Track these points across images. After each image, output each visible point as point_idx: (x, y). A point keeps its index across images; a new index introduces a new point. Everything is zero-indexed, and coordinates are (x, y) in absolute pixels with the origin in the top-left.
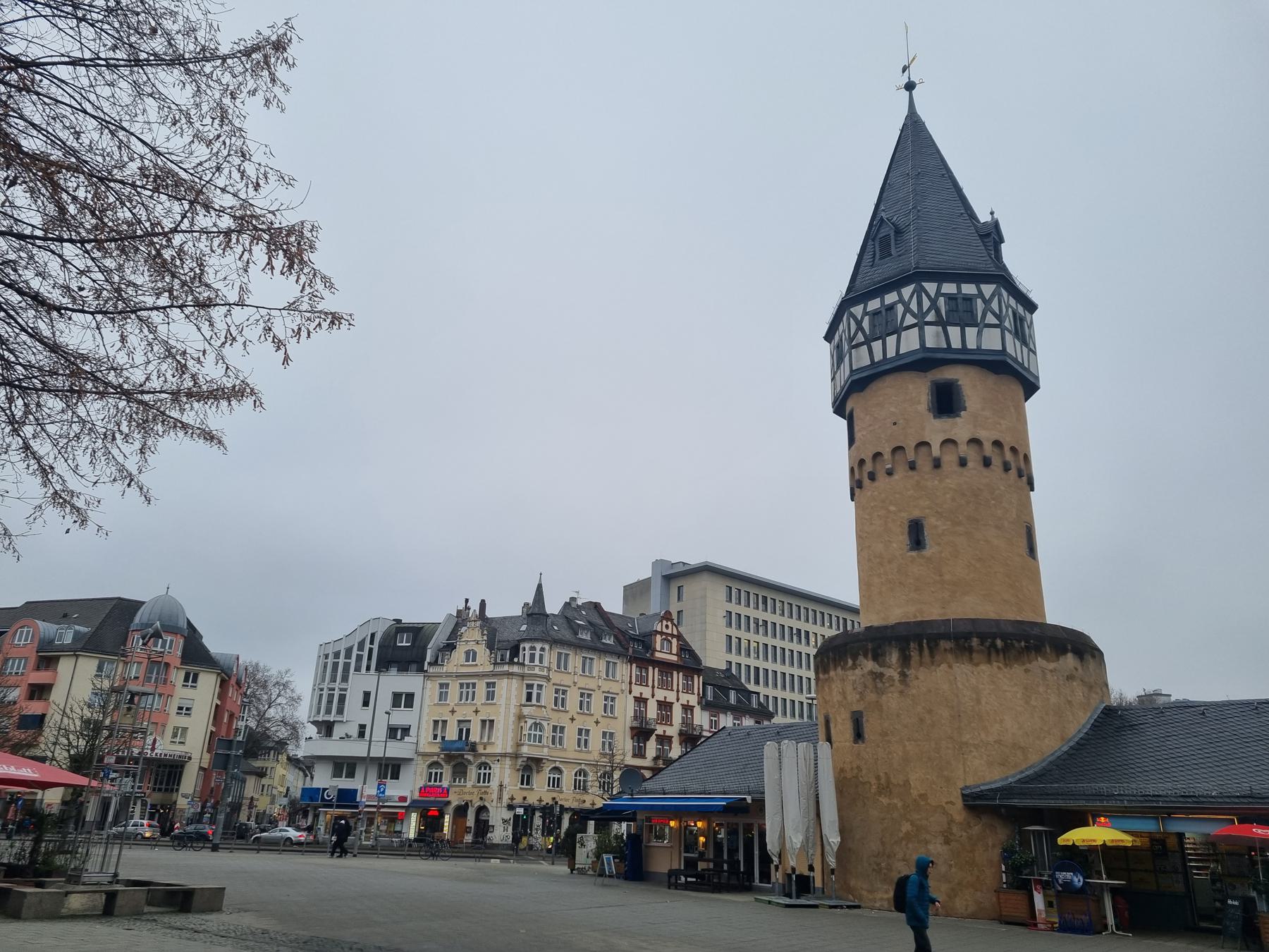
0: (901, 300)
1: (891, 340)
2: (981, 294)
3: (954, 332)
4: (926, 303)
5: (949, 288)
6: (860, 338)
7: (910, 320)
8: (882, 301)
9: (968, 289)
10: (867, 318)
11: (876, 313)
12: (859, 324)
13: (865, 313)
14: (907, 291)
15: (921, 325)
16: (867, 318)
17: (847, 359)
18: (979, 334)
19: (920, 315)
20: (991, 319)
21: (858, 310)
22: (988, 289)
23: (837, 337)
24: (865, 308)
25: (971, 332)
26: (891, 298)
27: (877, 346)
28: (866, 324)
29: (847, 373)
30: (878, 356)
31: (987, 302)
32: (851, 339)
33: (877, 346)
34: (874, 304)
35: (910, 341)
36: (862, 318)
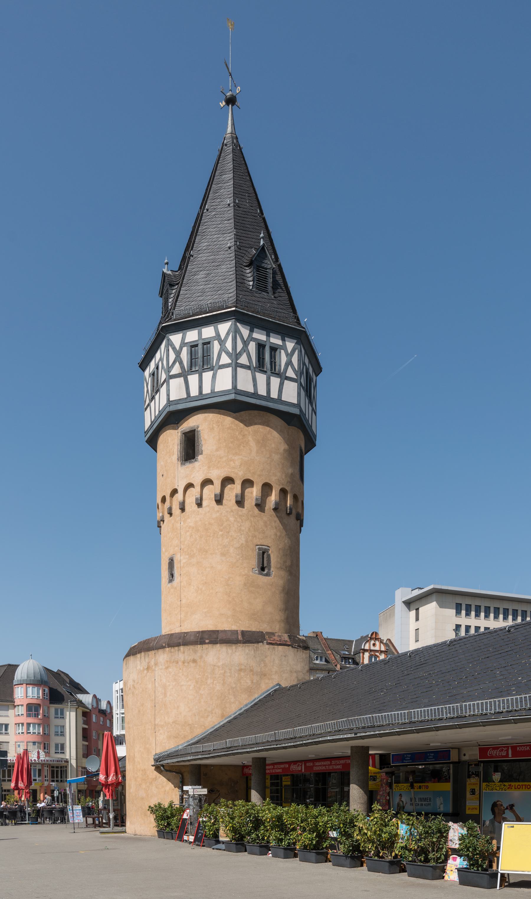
0: (218, 336)
1: (207, 376)
2: (284, 347)
3: (261, 378)
5: (260, 336)
6: (176, 370)
7: (225, 359)
8: (200, 334)
9: (276, 340)
10: (185, 349)
11: (193, 346)
12: (178, 353)
13: (183, 344)
15: (236, 366)
16: (185, 349)
17: (163, 390)
18: (281, 385)
20: (290, 373)
21: (176, 339)
22: (290, 345)
24: (183, 338)
25: (275, 381)
26: (208, 332)
27: (193, 379)
28: (185, 355)
29: (164, 402)
30: (194, 392)
31: (290, 356)
32: (169, 368)
33: (193, 379)
34: (192, 336)
35: (224, 381)
36: (181, 348)
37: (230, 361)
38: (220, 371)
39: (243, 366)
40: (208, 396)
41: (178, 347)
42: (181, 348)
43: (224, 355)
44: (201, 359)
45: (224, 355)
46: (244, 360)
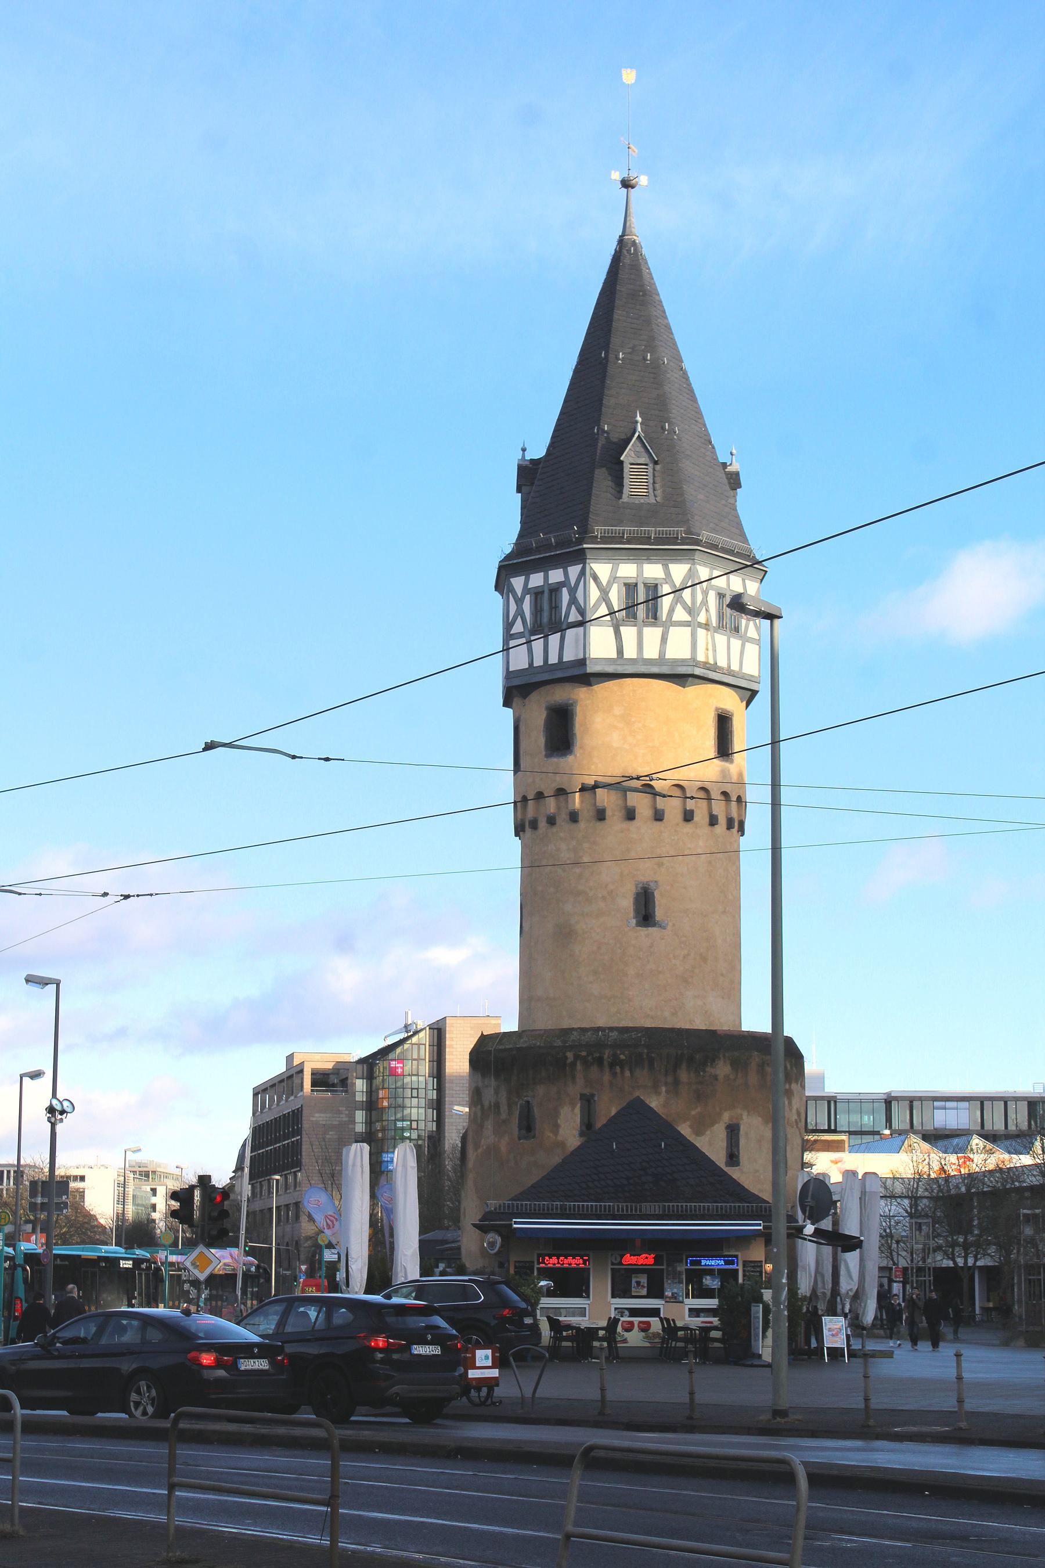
1: (652, 634)
3: (721, 639)
4: (699, 597)
7: (680, 614)
8: (640, 571)
10: (615, 587)
13: (613, 579)
14: (679, 571)
15: (692, 624)
19: (690, 611)
23: (536, 580)
24: (614, 570)
25: (736, 643)
26: (653, 571)
30: (630, 652)
33: (629, 633)
34: (628, 570)
35: (679, 647)
37: (689, 619)
38: (673, 630)
39: (700, 625)
40: (650, 662)
41: (604, 581)
42: (610, 584)
43: (679, 608)
44: (642, 605)
45: (679, 608)
46: (702, 618)
